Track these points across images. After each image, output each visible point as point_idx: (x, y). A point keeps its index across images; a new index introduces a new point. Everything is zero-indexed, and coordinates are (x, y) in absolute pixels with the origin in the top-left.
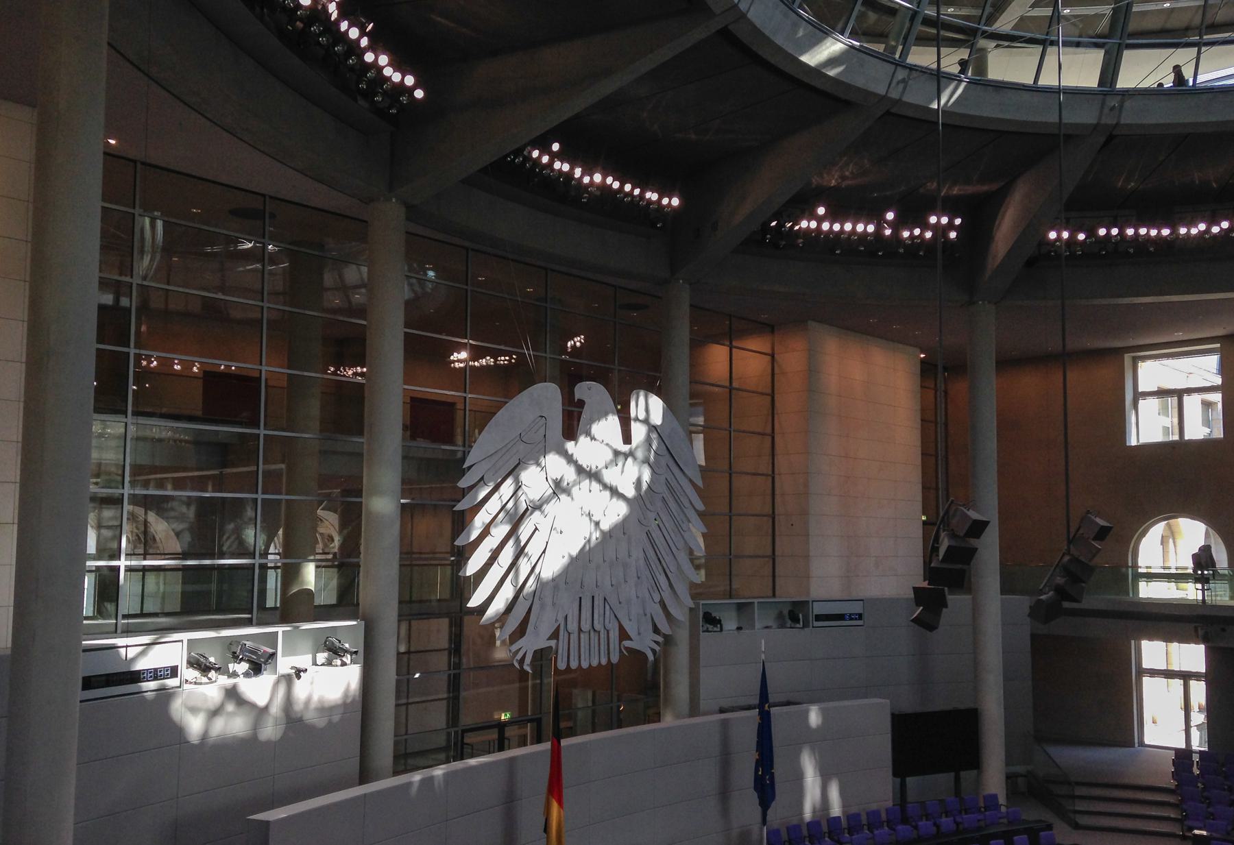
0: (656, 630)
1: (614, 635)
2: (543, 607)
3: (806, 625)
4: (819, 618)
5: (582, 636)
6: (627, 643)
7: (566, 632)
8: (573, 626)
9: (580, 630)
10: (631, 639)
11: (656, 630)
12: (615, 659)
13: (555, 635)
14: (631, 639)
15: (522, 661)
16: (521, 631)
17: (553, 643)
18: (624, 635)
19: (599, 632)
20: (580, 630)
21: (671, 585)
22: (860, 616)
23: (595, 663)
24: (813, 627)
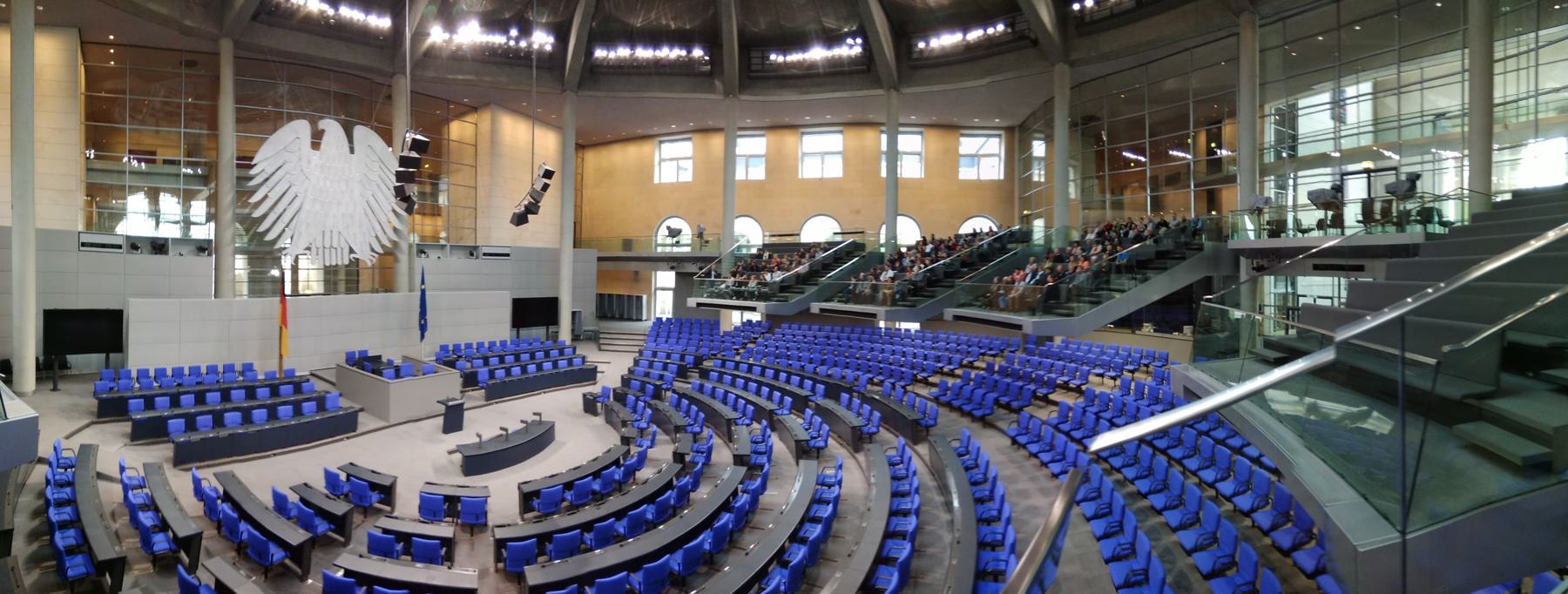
0: (373, 250)
1: (346, 251)
5: (326, 250)
6: (353, 255)
8: (320, 245)
9: (324, 247)
10: (355, 253)
11: (373, 250)
14: (355, 253)
18: (352, 251)
20: (324, 247)
21: (382, 228)
23: (334, 264)
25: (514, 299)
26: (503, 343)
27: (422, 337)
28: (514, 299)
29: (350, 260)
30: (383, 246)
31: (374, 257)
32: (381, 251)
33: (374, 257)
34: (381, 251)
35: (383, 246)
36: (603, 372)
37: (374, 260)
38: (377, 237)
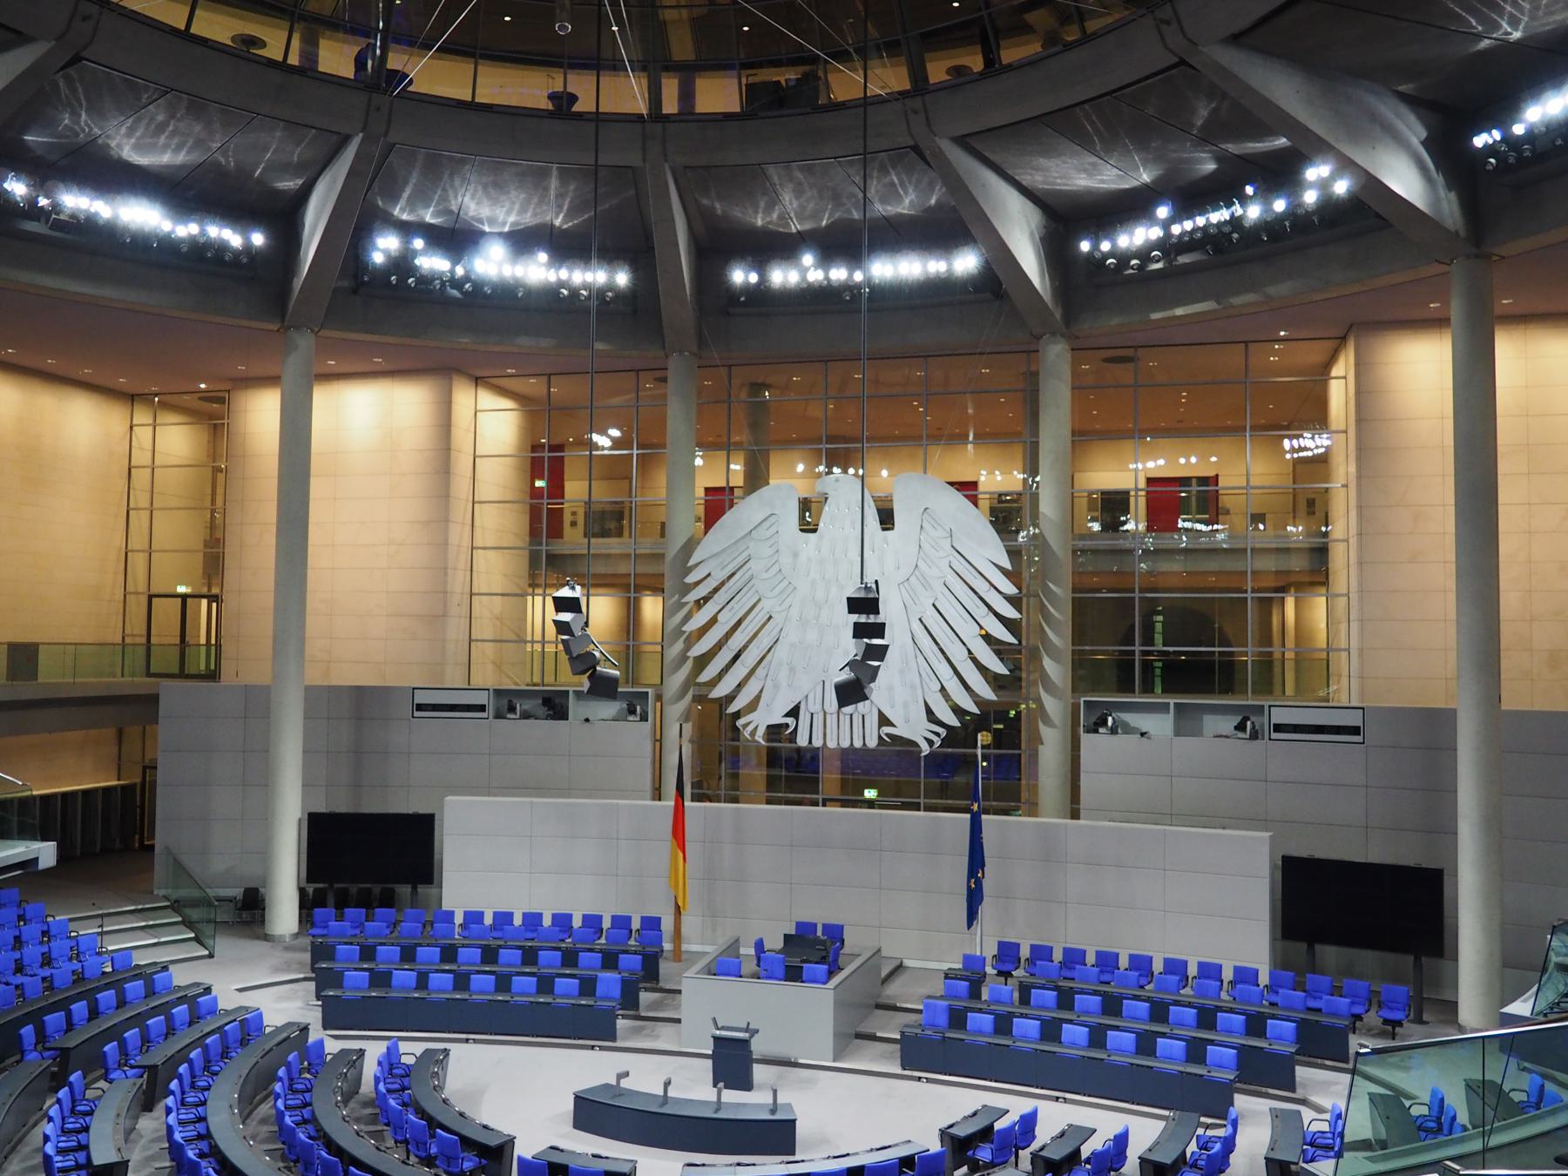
0: (931, 716)
2: (776, 687)
3: (1255, 736)
4: (1278, 728)
5: (828, 716)
7: (807, 713)
10: (892, 725)
12: (872, 743)
13: (794, 712)
14: (892, 725)
15: (753, 733)
16: (753, 706)
17: (790, 720)
18: (884, 721)
19: (851, 715)
20: (825, 713)
22: (1355, 731)
23: (845, 744)
24: (1270, 739)
25: (1287, 860)
26: (1245, 976)
27: (972, 916)
28: (1287, 860)
29: (880, 737)
30: (958, 711)
31: (937, 734)
32: (953, 721)
33: (937, 734)
34: (953, 721)
35: (958, 711)
36: (749, 1024)
37: (938, 742)
38: (943, 689)
